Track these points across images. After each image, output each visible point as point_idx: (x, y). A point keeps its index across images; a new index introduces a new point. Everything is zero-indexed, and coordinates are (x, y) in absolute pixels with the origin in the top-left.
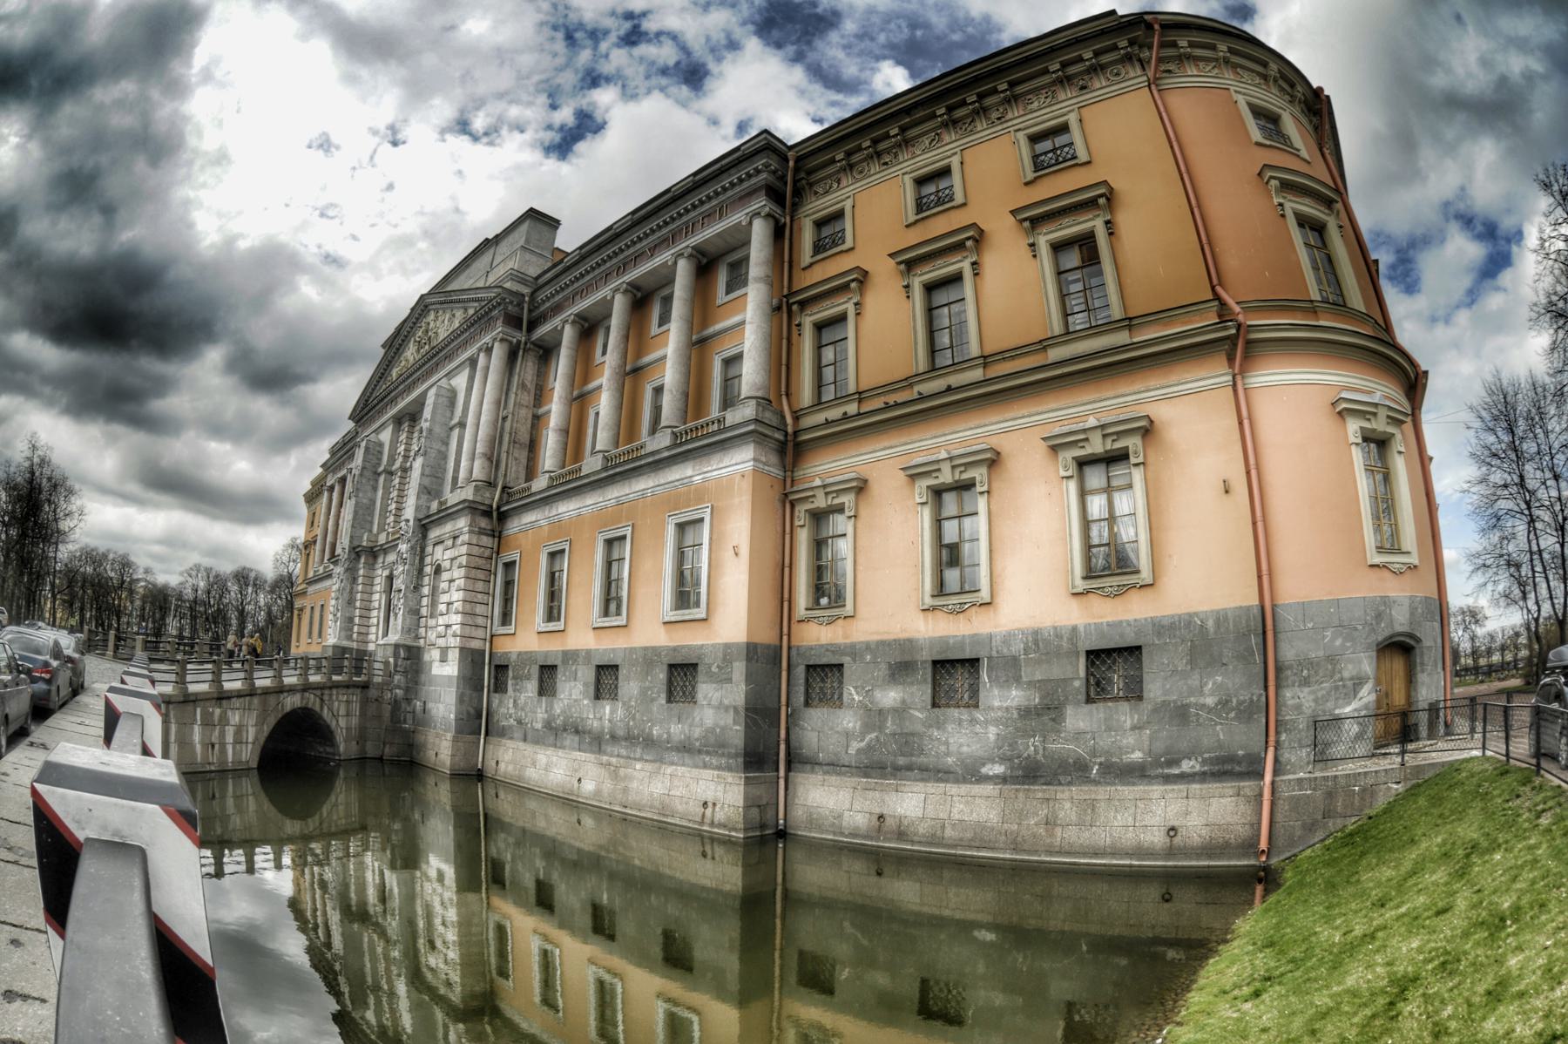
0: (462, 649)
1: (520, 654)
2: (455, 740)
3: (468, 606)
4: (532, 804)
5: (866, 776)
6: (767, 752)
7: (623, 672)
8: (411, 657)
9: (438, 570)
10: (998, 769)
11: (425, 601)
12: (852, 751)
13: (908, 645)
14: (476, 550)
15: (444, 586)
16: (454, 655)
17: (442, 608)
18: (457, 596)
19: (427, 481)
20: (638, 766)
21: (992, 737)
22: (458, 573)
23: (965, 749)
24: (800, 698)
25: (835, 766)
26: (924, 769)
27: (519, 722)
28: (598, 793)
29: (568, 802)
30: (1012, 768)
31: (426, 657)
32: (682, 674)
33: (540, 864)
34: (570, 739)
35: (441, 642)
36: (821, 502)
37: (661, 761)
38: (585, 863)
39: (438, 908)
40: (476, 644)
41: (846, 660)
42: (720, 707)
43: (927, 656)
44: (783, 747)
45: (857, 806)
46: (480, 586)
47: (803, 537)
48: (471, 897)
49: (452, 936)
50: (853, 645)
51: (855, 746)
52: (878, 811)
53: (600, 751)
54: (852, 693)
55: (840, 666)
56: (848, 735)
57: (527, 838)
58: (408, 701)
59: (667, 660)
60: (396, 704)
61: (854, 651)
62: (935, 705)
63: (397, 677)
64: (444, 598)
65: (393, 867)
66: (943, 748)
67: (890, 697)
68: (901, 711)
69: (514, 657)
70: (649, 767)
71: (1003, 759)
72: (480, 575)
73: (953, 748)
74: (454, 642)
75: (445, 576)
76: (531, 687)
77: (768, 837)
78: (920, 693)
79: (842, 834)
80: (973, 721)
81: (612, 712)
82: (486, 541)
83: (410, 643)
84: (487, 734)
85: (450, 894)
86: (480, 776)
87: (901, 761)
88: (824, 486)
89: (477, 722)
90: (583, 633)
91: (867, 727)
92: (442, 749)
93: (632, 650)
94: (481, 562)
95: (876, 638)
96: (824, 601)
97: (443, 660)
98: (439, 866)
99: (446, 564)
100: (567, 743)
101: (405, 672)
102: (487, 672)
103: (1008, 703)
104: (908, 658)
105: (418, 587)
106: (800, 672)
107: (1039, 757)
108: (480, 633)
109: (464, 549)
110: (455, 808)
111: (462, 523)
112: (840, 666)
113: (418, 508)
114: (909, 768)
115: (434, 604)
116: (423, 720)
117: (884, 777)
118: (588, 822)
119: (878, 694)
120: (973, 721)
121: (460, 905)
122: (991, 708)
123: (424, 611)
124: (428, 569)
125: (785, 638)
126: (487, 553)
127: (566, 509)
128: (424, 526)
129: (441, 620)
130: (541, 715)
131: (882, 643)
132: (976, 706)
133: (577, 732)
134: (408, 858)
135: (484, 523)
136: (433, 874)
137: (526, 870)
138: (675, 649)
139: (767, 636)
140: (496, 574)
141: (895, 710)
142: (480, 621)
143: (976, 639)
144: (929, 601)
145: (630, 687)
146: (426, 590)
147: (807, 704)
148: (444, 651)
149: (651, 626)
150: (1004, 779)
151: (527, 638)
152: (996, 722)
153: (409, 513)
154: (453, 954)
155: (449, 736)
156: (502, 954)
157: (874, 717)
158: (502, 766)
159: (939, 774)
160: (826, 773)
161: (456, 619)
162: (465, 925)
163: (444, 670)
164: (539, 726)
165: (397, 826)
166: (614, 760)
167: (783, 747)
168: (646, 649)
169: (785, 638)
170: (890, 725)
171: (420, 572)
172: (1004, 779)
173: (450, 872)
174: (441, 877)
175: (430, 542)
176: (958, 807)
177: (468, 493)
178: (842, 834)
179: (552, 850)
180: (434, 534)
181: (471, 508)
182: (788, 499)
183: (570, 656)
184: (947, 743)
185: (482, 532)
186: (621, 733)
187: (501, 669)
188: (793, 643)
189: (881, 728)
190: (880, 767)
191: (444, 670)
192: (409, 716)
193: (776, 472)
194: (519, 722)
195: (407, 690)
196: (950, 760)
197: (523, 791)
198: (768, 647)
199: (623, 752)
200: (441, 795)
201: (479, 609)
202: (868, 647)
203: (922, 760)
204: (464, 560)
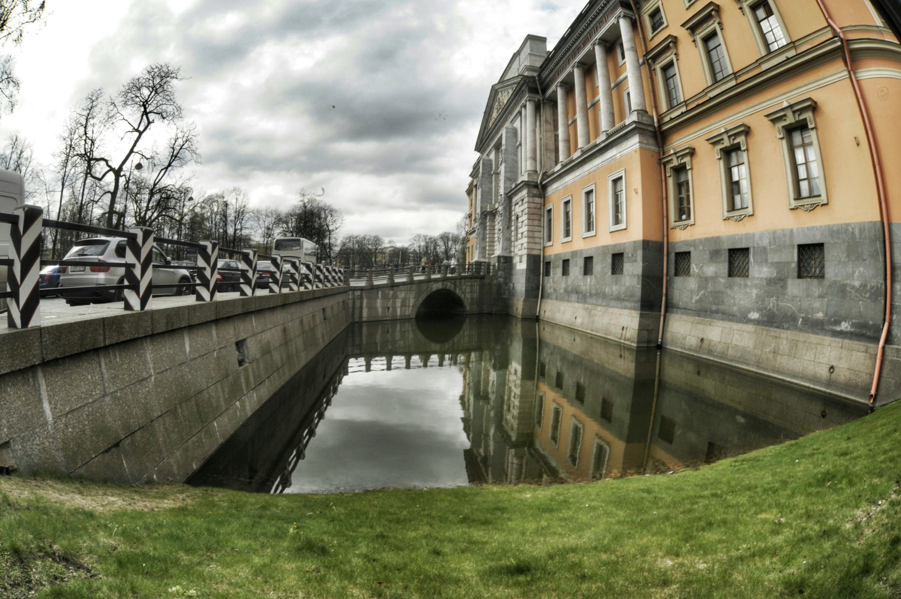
0: (528, 255)
1: (555, 255)
2: (525, 301)
3: (530, 234)
4: (557, 332)
5: (699, 316)
6: (654, 301)
7: (595, 260)
8: (507, 261)
9: (517, 218)
10: (755, 315)
11: (513, 234)
12: (693, 301)
13: (716, 240)
14: (532, 205)
15: (520, 225)
16: (525, 258)
17: (520, 235)
18: (525, 229)
19: (509, 175)
20: (599, 308)
21: (754, 296)
22: (525, 217)
23: (742, 302)
24: (672, 271)
25: (686, 310)
26: (724, 313)
27: (555, 290)
28: (582, 324)
29: (571, 330)
30: (762, 315)
31: (514, 261)
32: (617, 259)
33: (559, 364)
34: (574, 297)
35: (520, 253)
36: (675, 163)
37: (607, 306)
38: (576, 362)
39: (513, 388)
40: (535, 252)
41: (692, 249)
42: (633, 275)
43: (727, 246)
44: (664, 298)
45: (692, 334)
46: (536, 223)
47: (671, 182)
48: (529, 383)
49: (517, 402)
50: (694, 241)
51: (695, 298)
52: (701, 336)
53: (585, 302)
54: (694, 268)
55: (689, 253)
56: (692, 292)
57: (557, 350)
58: (506, 284)
59: (612, 252)
60: (499, 286)
61: (694, 243)
62: (730, 275)
63: (500, 273)
64: (520, 231)
65: (495, 368)
66: (732, 301)
67: (710, 270)
68: (714, 278)
69: (553, 257)
70: (603, 309)
71: (759, 310)
72: (536, 217)
73: (737, 301)
74: (525, 252)
75: (520, 220)
76: (560, 271)
77: (651, 347)
78: (724, 268)
79: (685, 348)
80: (746, 285)
81: (591, 281)
82: (537, 200)
83: (506, 255)
84: (542, 298)
85: (518, 382)
86: (537, 319)
87: (714, 308)
88: (675, 153)
89: (535, 291)
90: (580, 243)
91: (700, 288)
92: (519, 306)
93: (598, 248)
94: (535, 211)
95: (704, 236)
96: (684, 217)
97: (521, 262)
98: (516, 366)
99: (520, 214)
100: (573, 299)
101: (504, 270)
102: (539, 266)
103: (761, 276)
104: (718, 248)
105: (509, 227)
106: (673, 256)
107: (775, 310)
108: (538, 247)
109: (526, 206)
110: (523, 335)
111: (524, 192)
112: (689, 253)
113: (505, 188)
114: (717, 312)
115: (517, 234)
116: (512, 293)
117: (705, 317)
118: (578, 339)
119: (705, 269)
120: (746, 285)
121: (522, 386)
122: (754, 278)
123: (513, 239)
124: (513, 218)
125: (665, 238)
126: (539, 206)
127: (569, 179)
128: (509, 197)
129: (520, 242)
130: (563, 285)
131: (707, 239)
132: (747, 276)
133: (577, 293)
134: (502, 364)
135: (535, 191)
136: (513, 371)
137: (553, 367)
138: (615, 246)
139: (655, 237)
140: (541, 216)
141: (712, 278)
142: (537, 240)
143: (749, 237)
144: (726, 215)
145: (597, 267)
146: (513, 228)
147: (676, 274)
148: (521, 256)
149: (606, 237)
150: (757, 322)
151: (557, 248)
152: (756, 286)
153: (502, 191)
154: (515, 412)
155: (522, 299)
156: (540, 413)
157: (704, 280)
158: (547, 313)
159: (729, 316)
160: (682, 313)
161: (525, 240)
162: (523, 397)
163: (521, 266)
164: (562, 291)
165: (498, 347)
166: (590, 306)
167: (664, 298)
168: (603, 247)
169: (665, 238)
170: (710, 287)
171: (510, 219)
172: (757, 322)
173: (520, 369)
174: (516, 371)
175: (513, 204)
176: (736, 336)
177: (525, 178)
178: (685, 348)
179: (563, 355)
180: (515, 199)
181: (527, 184)
182: (662, 163)
183: (574, 254)
184: (734, 298)
185: (534, 196)
186: (593, 292)
187: (548, 264)
188: (670, 241)
189: (706, 288)
190: (706, 311)
191: (521, 266)
192: (507, 292)
193: (654, 148)
194: (555, 290)
195: (505, 278)
196: (735, 308)
197: (554, 325)
198: (656, 242)
199: (594, 302)
200: (518, 329)
201: (537, 234)
202: (700, 240)
203: (722, 307)
204: (526, 211)
